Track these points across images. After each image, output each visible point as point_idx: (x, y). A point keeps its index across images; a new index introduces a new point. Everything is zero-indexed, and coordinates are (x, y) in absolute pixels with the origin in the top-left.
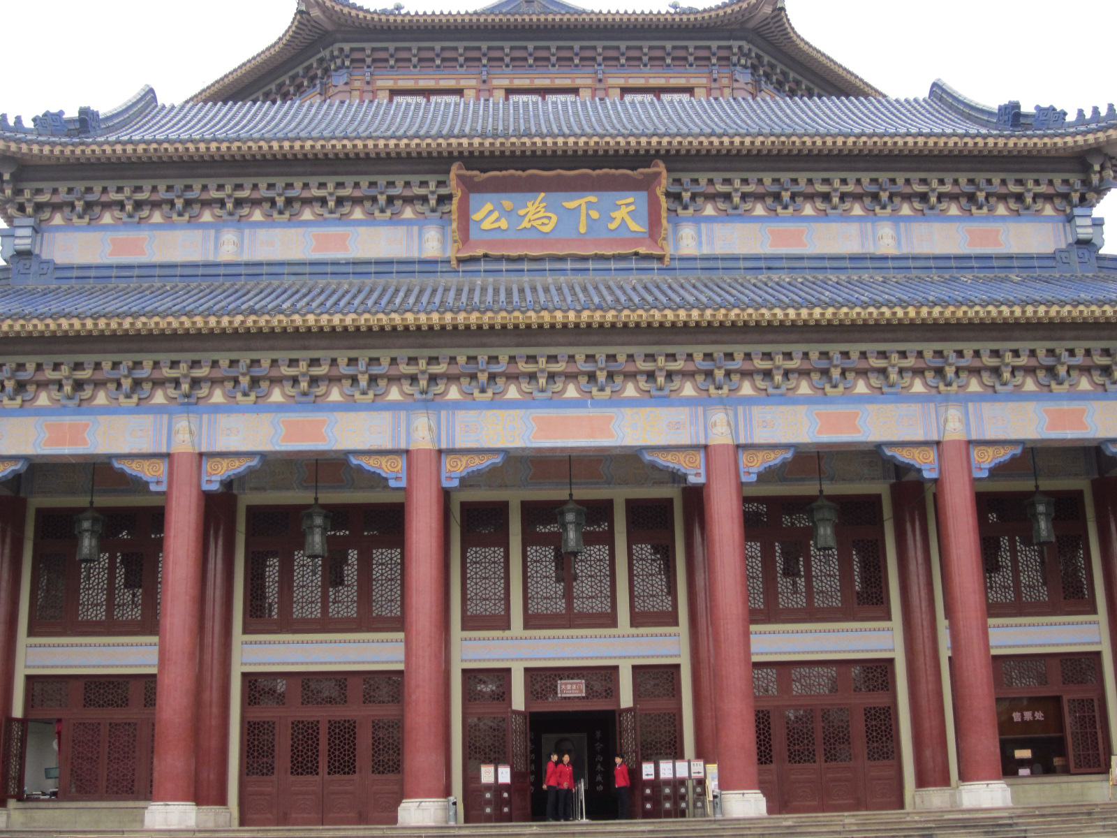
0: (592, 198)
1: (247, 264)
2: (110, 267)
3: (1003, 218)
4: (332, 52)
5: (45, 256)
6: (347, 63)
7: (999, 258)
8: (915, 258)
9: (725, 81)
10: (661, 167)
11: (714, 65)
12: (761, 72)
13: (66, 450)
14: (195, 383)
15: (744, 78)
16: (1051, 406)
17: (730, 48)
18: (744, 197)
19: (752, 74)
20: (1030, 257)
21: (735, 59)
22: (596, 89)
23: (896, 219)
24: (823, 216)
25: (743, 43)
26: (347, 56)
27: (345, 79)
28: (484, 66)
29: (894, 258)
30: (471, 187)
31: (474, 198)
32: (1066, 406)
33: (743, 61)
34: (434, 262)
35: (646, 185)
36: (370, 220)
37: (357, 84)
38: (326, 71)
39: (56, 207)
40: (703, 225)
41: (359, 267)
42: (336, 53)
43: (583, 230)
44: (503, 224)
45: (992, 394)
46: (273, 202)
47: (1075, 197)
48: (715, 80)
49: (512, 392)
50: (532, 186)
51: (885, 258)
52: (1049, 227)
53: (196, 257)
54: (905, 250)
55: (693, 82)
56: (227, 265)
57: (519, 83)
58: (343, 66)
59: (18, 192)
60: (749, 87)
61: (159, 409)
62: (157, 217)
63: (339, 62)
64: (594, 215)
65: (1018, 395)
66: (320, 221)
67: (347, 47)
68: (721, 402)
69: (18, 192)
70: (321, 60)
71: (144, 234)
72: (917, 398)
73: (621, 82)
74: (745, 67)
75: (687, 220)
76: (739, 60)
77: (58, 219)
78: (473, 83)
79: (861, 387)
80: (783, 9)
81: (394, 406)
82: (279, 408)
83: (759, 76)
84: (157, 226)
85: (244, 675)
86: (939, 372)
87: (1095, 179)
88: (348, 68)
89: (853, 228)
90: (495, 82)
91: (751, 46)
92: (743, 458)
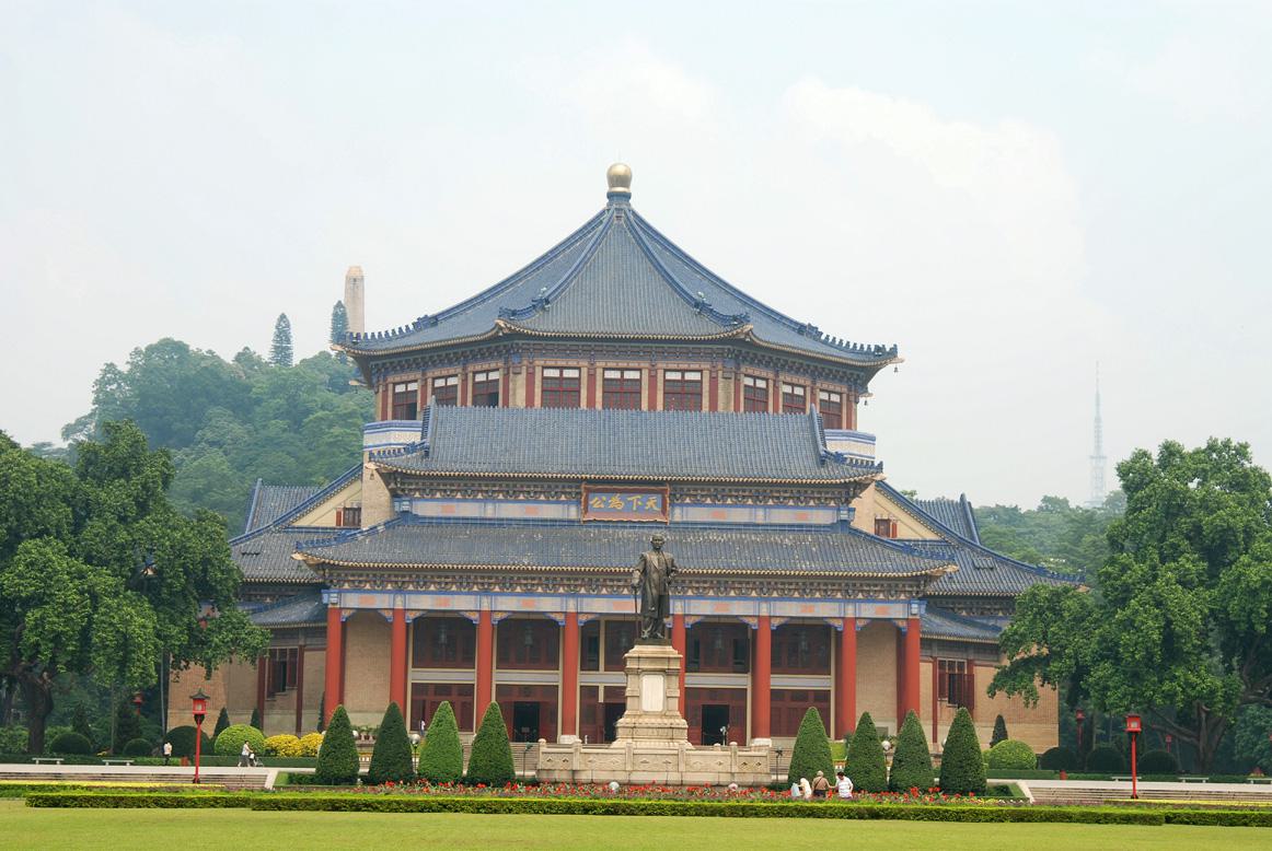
0: (639, 497)
1: (498, 519)
2: (441, 518)
3: (811, 507)
5: (414, 513)
7: (807, 526)
8: (771, 525)
9: (720, 367)
10: (668, 487)
13: (443, 608)
14: (489, 584)
15: (731, 365)
16: (804, 604)
17: (723, 349)
18: (702, 496)
20: (820, 526)
23: (766, 507)
24: (735, 505)
25: (729, 347)
29: (763, 525)
30: (589, 491)
31: (591, 495)
32: (808, 604)
34: (573, 521)
35: (662, 492)
36: (548, 502)
37: (525, 362)
39: (416, 490)
40: (685, 508)
41: (544, 523)
43: (635, 508)
44: (602, 506)
45: (781, 599)
46: (508, 492)
47: (843, 500)
49: (604, 591)
50: (615, 491)
51: (758, 525)
52: (830, 512)
53: (477, 515)
54: (768, 521)
55: (703, 367)
56: (490, 519)
57: (610, 365)
59: (402, 484)
61: (476, 593)
62: (459, 496)
64: (640, 503)
65: (791, 599)
66: (527, 501)
67: (520, 342)
68: (680, 598)
69: (402, 484)
70: (505, 346)
71: (455, 504)
72: (753, 599)
73: (664, 366)
75: (678, 505)
77: (417, 495)
79: (732, 594)
81: (561, 595)
82: (519, 594)
84: (459, 500)
85: (497, 685)
86: (761, 589)
87: (851, 493)
89: (747, 511)
92: (687, 619)
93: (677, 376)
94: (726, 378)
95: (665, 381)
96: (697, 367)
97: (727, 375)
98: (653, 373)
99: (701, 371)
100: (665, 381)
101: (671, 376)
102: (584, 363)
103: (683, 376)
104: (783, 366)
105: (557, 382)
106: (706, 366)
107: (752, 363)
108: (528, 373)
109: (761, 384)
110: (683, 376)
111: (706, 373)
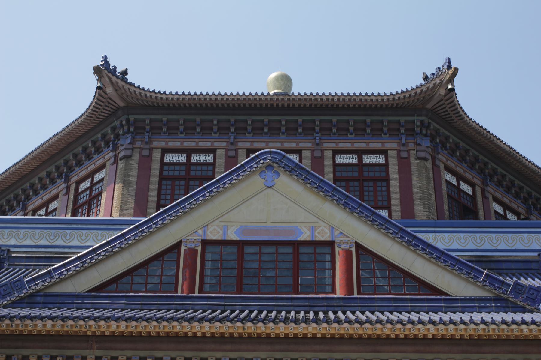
4: (121, 122)
6: (132, 129)
9: (411, 146)
11: (403, 134)
12: (438, 141)
15: (426, 143)
19: (431, 141)
21: (418, 130)
22: (314, 150)
26: (132, 125)
27: (129, 140)
28: (232, 133)
33: (424, 132)
37: (138, 144)
38: (117, 137)
42: (124, 122)
48: (404, 145)
58: (129, 131)
60: (430, 150)
63: (126, 128)
73: (333, 146)
74: (426, 135)
76: (421, 130)
78: (224, 144)
80: (453, 90)
83: (436, 143)
88: (132, 133)
90: (240, 144)
91: (430, 121)
93: (352, 159)
94: (418, 158)
95: (335, 166)
96: (377, 145)
97: (422, 154)
98: (318, 154)
99: (384, 152)
100: (335, 166)
101: (342, 159)
102: (220, 144)
103: (360, 159)
104: (491, 177)
105: (183, 168)
106: (391, 145)
107: (452, 153)
108: (141, 156)
109: (465, 188)
110: (360, 159)
111: (392, 154)
